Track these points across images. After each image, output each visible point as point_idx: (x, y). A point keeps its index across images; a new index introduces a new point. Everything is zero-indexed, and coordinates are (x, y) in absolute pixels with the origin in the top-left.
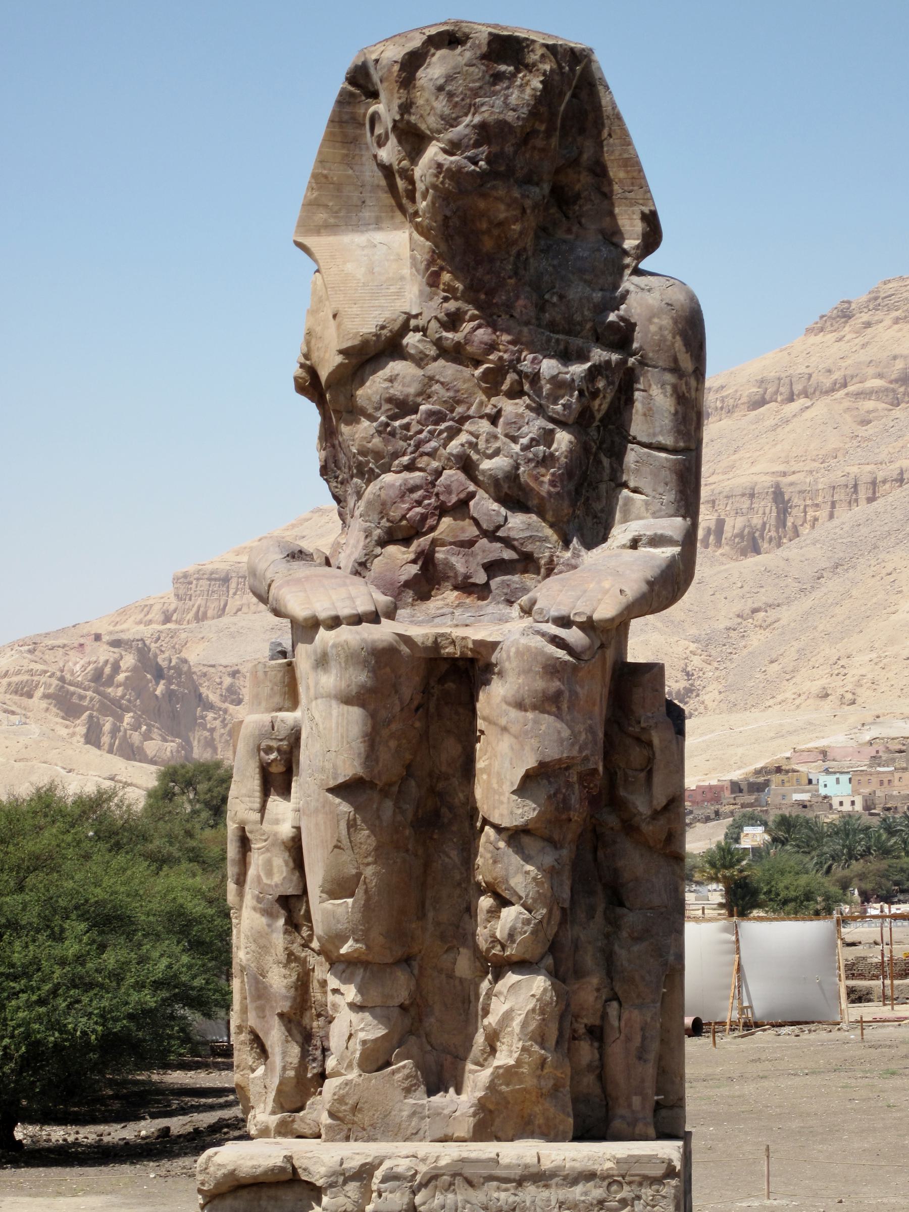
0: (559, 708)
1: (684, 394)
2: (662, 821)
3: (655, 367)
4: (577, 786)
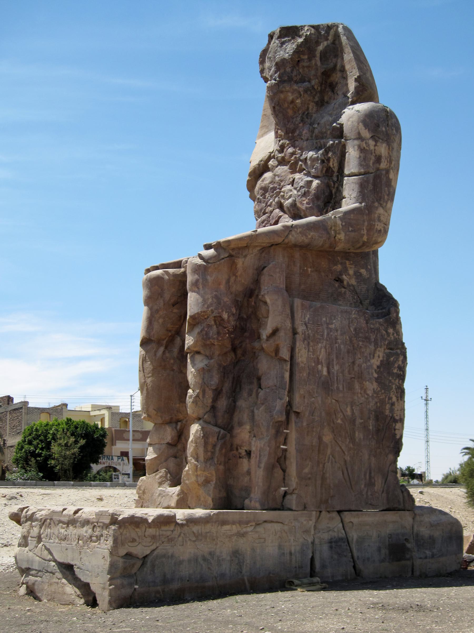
0: (198, 288)
1: (364, 148)
2: (271, 341)
3: (350, 140)
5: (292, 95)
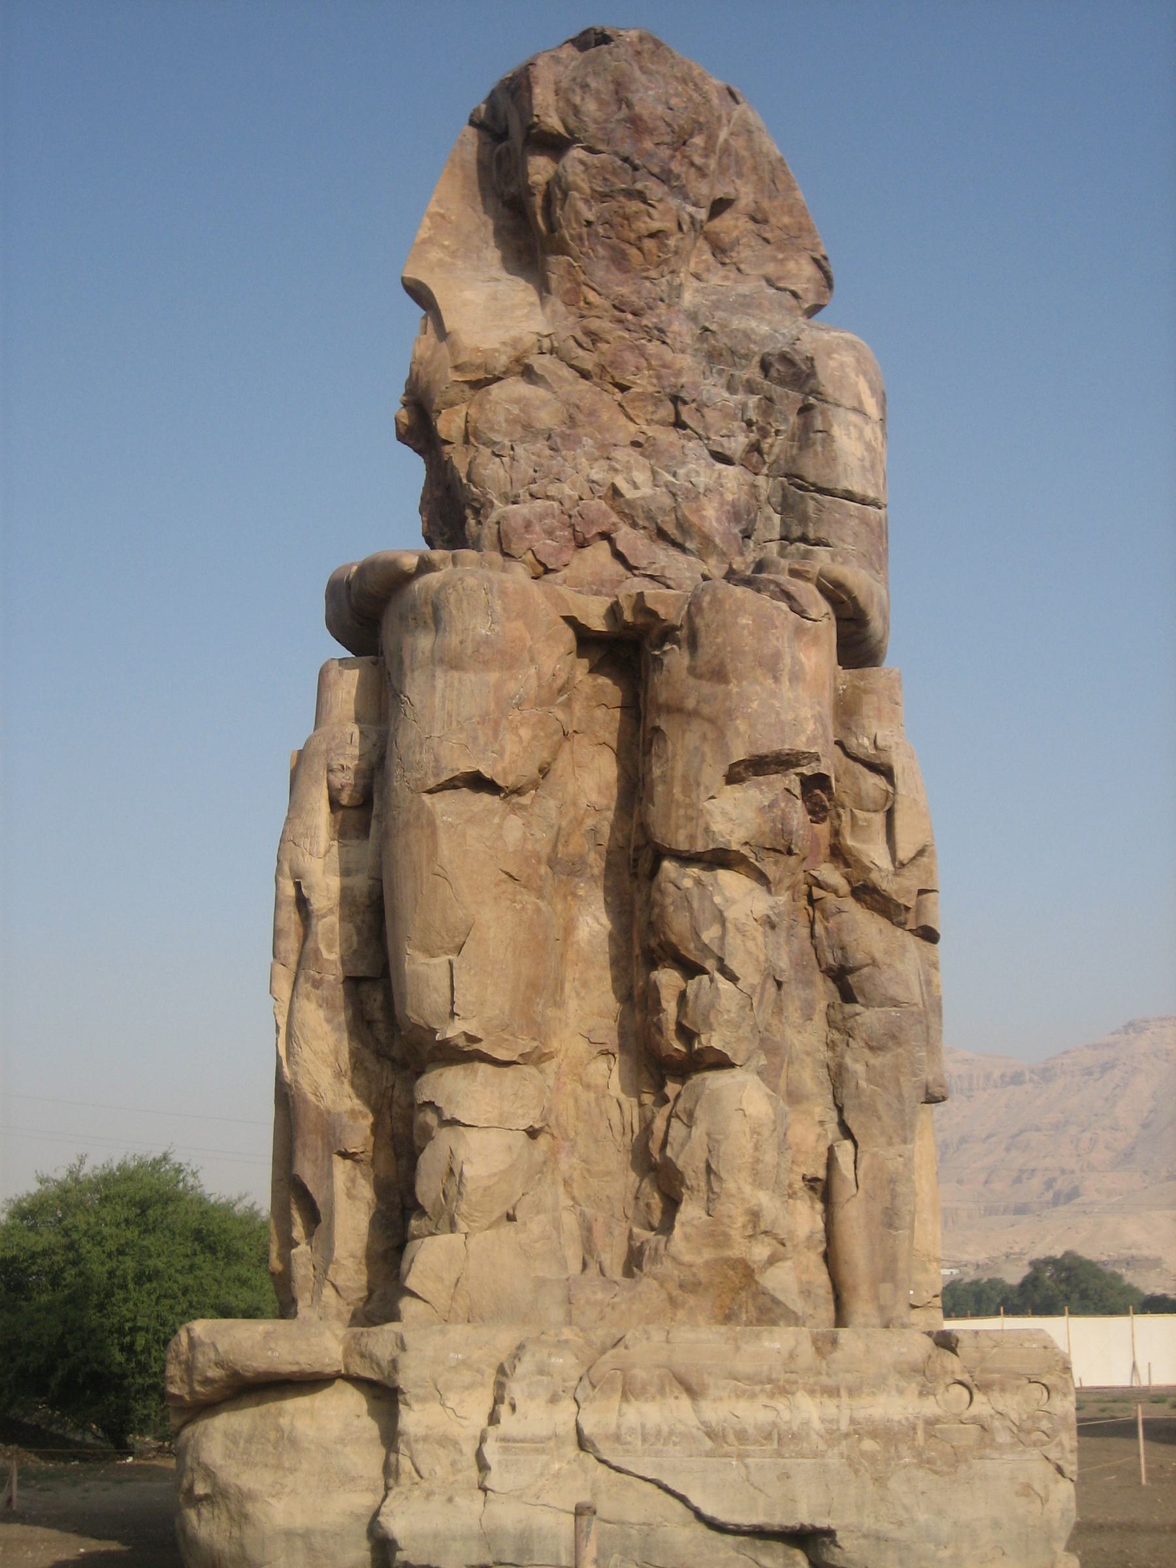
0: (776, 679)
4: (799, 802)
5: (661, 220)
